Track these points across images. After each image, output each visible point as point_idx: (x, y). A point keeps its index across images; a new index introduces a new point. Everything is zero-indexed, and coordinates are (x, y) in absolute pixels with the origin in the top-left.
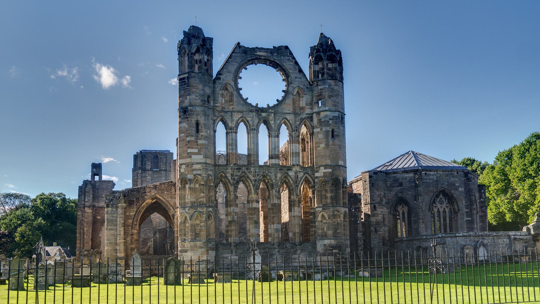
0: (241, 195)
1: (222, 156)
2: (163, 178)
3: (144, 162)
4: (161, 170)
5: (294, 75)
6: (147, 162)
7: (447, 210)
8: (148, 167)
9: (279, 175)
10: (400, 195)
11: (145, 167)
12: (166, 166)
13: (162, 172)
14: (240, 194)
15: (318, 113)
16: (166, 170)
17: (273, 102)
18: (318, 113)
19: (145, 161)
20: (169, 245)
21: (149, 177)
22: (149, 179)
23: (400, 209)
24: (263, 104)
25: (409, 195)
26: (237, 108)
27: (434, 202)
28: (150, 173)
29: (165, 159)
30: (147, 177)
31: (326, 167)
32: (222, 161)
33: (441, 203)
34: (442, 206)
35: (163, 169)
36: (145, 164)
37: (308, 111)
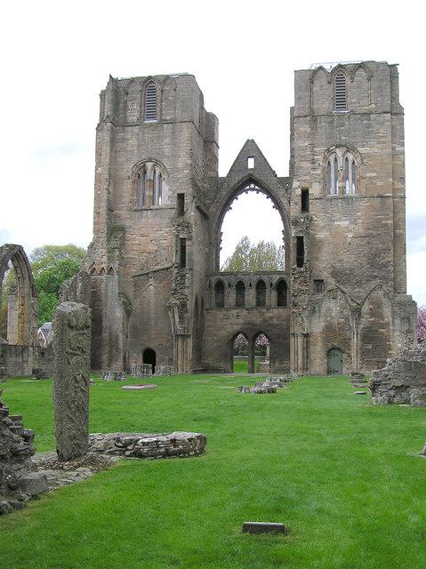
0: (374, 174)
1: (321, 71)
2: (167, 140)
3: (122, 105)
4: (162, 122)
6: (129, 104)
8: (133, 116)
11: (125, 118)
12: (175, 109)
13: (165, 126)
14: (371, 172)
16: (173, 122)
19: (126, 102)
20: (176, 310)
21: (133, 142)
22: (132, 146)
28: (136, 130)
29: (172, 92)
30: (128, 140)
32: (322, 86)
35: (168, 118)
36: (126, 108)
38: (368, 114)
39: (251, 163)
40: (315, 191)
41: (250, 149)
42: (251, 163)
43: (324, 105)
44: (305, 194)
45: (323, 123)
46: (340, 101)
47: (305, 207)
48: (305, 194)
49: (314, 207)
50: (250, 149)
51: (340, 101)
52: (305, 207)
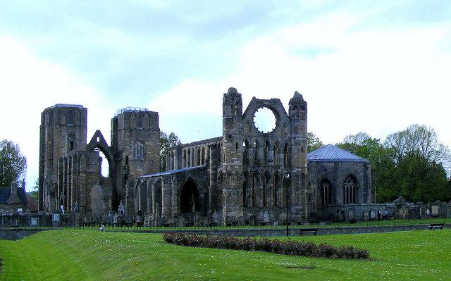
4: (75, 126)
5: (282, 115)
7: (353, 187)
9: (274, 171)
10: (325, 176)
15: (295, 138)
16: (80, 126)
17: (271, 130)
18: (295, 138)
23: (324, 185)
24: (265, 132)
25: (330, 178)
26: (253, 134)
27: (345, 182)
31: (298, 168)
33: (349, 182)
34: (350, 184)
37: (289, 136)
38: (148, 130)
39: (98, 140)
40: (131, 157)
41: (98, 133)
42: (98, 140)
43: (134, 125)
44: (127, 157)
45: (133, 132)
46: (140, 124)
47: (127, 163)
48: (127, 157)
49: (130, 163)
50: (98, 133)
51: (140, 124)
52: (127, 163)
